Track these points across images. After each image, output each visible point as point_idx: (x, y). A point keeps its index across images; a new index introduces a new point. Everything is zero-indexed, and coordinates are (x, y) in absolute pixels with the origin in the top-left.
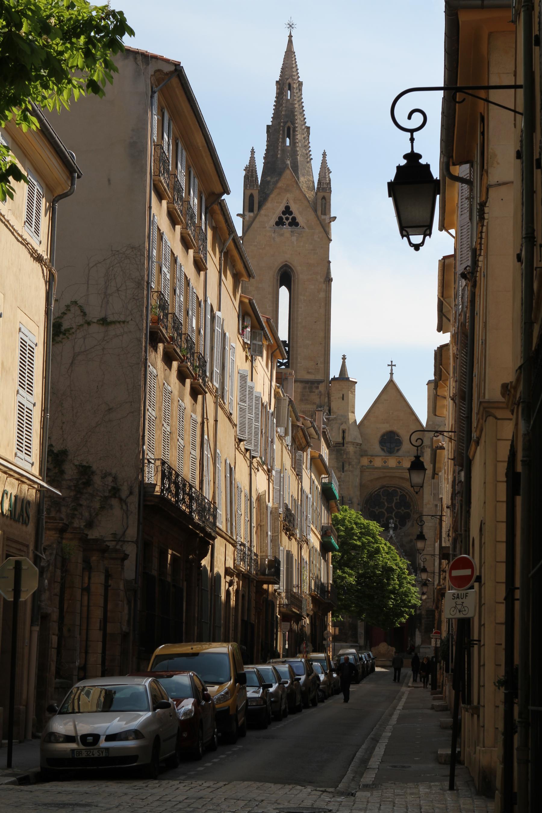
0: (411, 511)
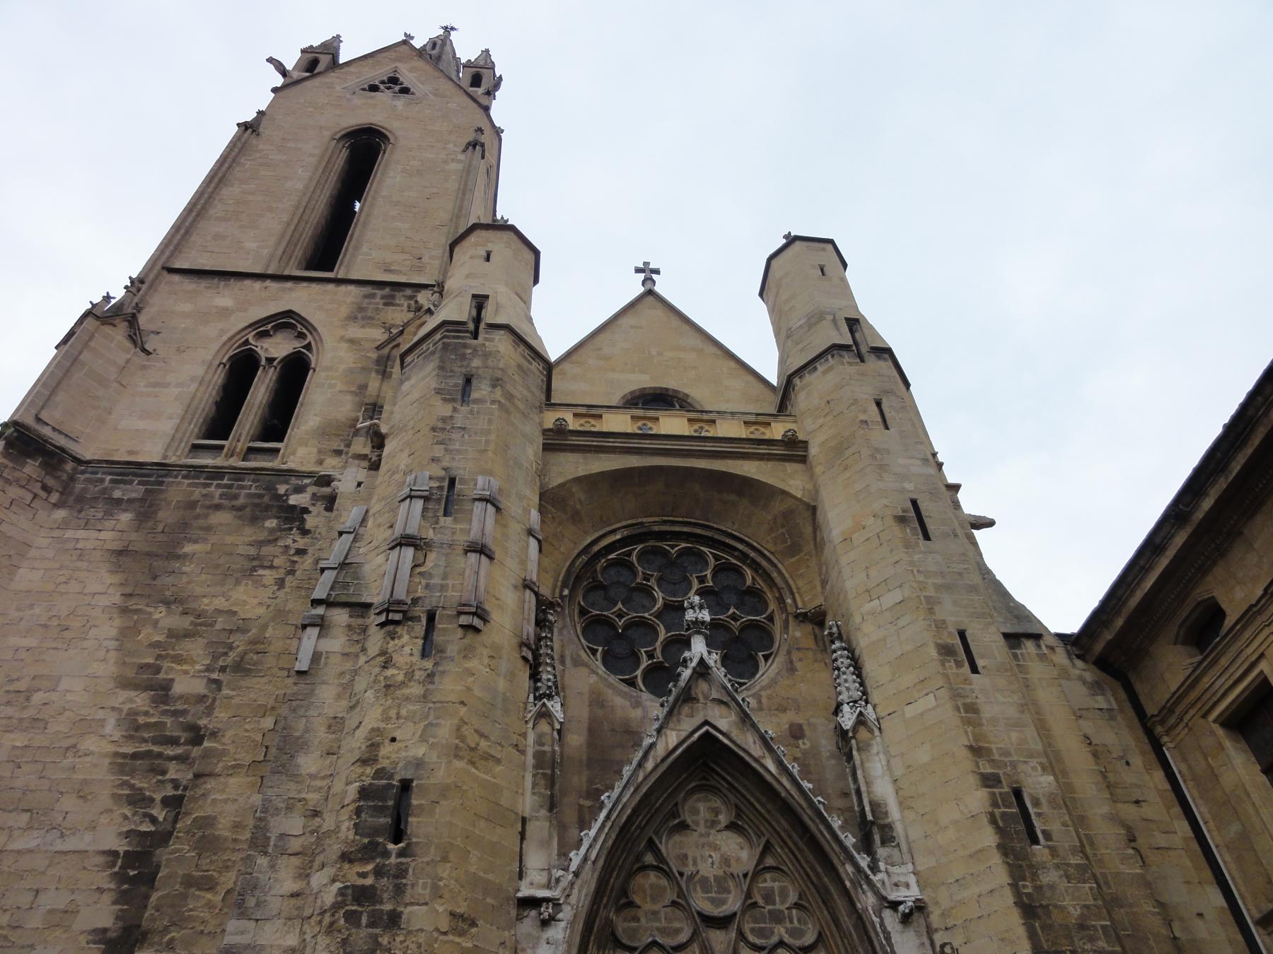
0: (771, 619)
